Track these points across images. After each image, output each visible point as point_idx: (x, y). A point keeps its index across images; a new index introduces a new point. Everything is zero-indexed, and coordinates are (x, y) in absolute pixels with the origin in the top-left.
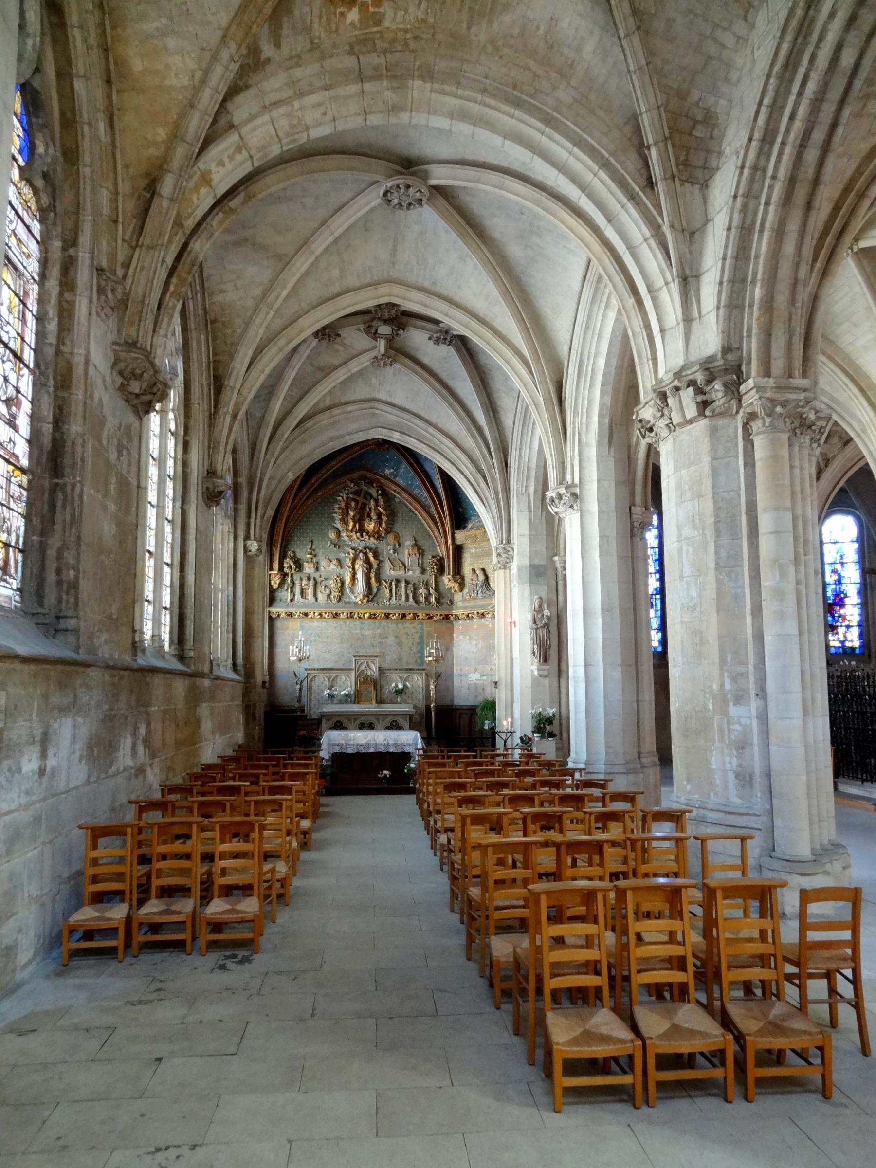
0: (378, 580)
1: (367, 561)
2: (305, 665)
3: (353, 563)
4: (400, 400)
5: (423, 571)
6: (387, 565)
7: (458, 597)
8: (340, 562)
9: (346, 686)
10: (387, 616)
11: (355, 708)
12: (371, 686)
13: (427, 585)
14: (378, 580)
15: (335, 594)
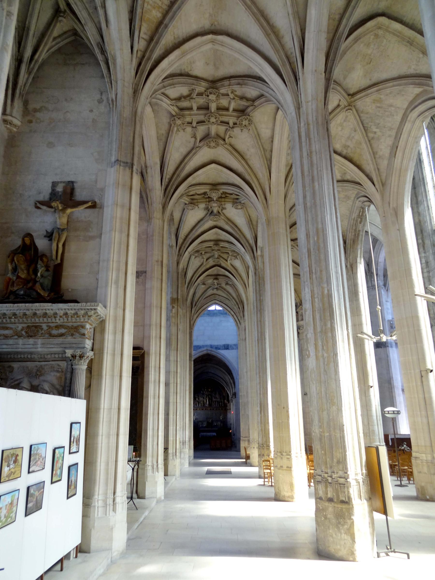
0: (212, 401)
1: (209, 397)
2: (197, 420)
3: (206, 397)
4: (212, 372)
5: (221, 399)
6: (213, 398)
7: (228, 404)
8: (204, 398)
9: (205, 424)
10: (213, 409)
11: (207, 429)
12: (210, 425)
13: (222, 403)
14: (212, 402)
15: (202, 405)
